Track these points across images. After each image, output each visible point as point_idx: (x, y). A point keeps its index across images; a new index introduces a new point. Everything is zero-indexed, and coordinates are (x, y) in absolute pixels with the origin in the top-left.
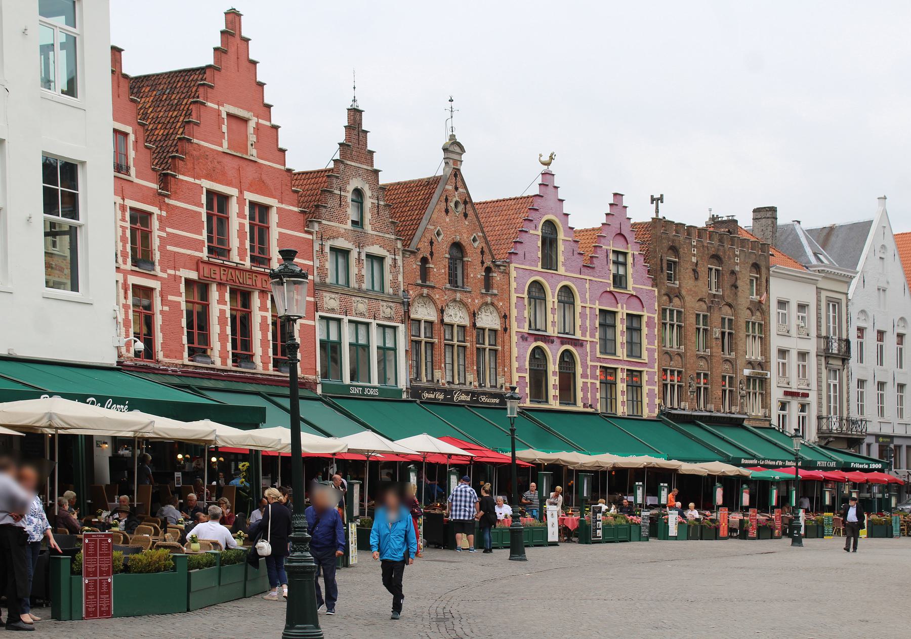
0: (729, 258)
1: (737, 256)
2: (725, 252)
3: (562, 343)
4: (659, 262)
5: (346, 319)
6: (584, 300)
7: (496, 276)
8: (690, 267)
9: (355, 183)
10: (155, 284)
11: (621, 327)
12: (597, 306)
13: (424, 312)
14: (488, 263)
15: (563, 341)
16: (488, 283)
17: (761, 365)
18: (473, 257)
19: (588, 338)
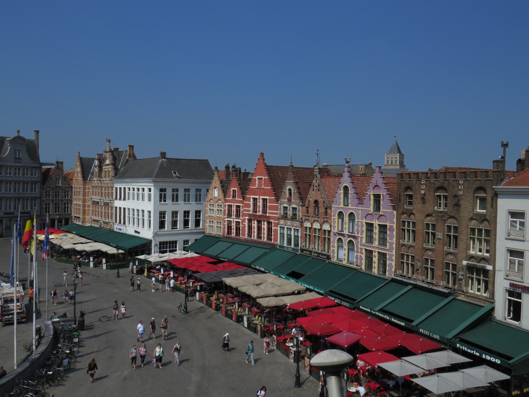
0: (453, 187)
1: (460, 184)
2: (449, 184)
3: (349, 237)
4: (398, 196)
5: (285, 227)
6: (358, 219)
7: (329, 211)
8: (419, 197)
9: (288, 187)
10: (240, 221)
11: (376, 230)
12: (364, 221)
13: (308, 225)
14: (326, 206)
15: (349, 236)
16: (326, 213)
17: (483, 259)
18: (321, 205)
19: (359, 235)
